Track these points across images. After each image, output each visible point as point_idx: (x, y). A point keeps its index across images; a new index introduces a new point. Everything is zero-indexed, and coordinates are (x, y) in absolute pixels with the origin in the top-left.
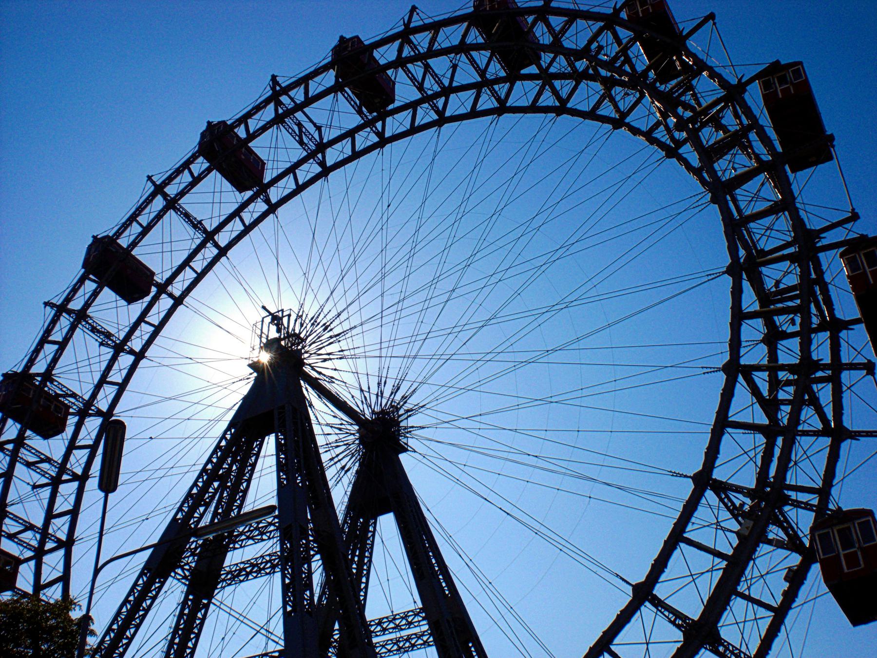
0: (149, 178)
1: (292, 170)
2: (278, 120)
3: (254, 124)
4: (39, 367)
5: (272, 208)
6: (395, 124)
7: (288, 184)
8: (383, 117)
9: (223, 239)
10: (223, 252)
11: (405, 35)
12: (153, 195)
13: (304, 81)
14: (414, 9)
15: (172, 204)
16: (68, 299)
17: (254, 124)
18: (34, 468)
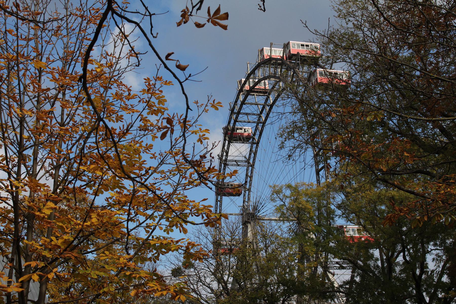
0: (218, 155)
2: (236, 121)
3: (231, 125)
5: (258, 143)
10: (253, 166)
12: (221, 163)
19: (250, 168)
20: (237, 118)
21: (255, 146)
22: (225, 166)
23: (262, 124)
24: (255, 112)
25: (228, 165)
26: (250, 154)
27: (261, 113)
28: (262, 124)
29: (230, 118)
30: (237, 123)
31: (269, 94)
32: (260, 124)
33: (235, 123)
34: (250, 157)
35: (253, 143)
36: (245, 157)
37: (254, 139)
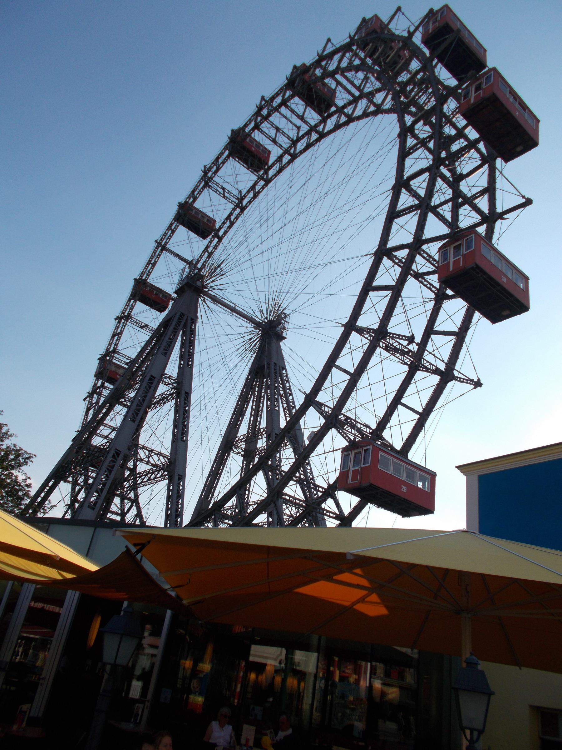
0: (205, 167)
1: (280, 158)
2: (257, 127)
3: (247, 130)
4: (144, 278)
5: (268, 182)
6: (330, 123)
7: (276, 168)
8: (324, 121)
9: (245, 202)
10: (243, 209)
11: (317, 63)
13: (273, 98)
14: (329, 40)
15: (207, 185)
16: (162, 239)
17: (247, 130)
18: (145, 329)
19: (238, 210)
20: (261, 122)
21: (262, 183)
22: (204, 187)
23: (289, 158)
24: (291, 136)
25: (209, 187)
26: (248, 192)
27: (299, 139)
28: (289, 158)
29: (250, 120)
30: (256, 131)
31: (330, 116)
32: (287, 156)
33: (253, 130)
34: (245, 196)
35: (261, 178)
36: (240, 192)
37: (266, 172)
